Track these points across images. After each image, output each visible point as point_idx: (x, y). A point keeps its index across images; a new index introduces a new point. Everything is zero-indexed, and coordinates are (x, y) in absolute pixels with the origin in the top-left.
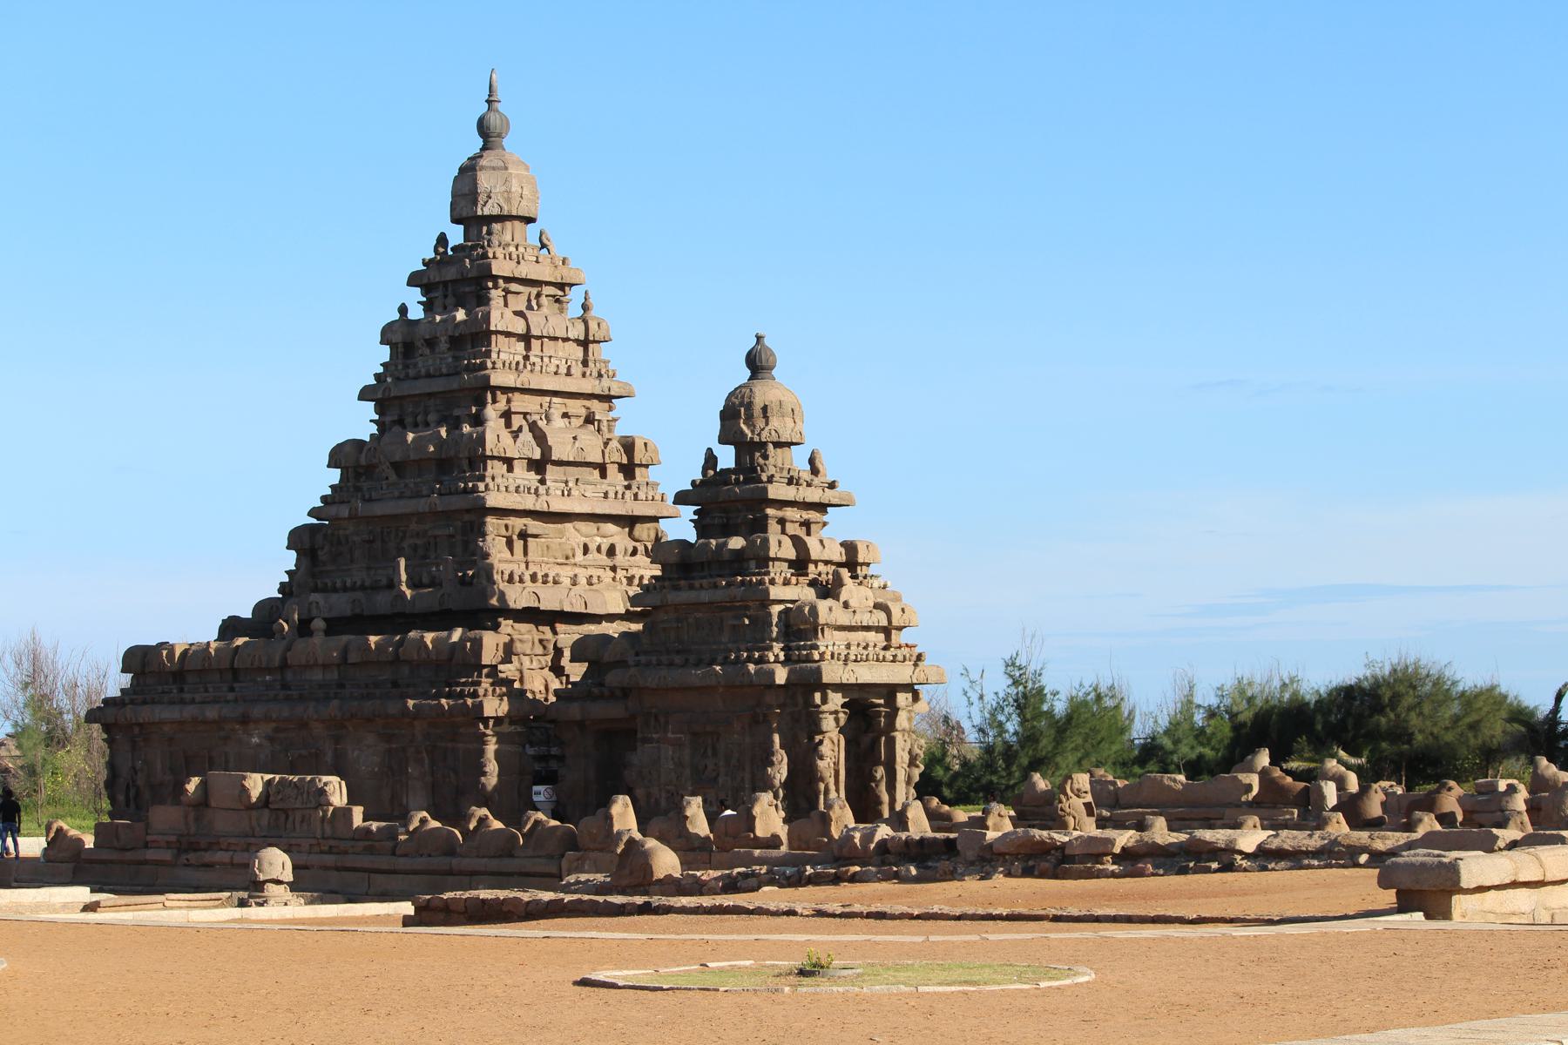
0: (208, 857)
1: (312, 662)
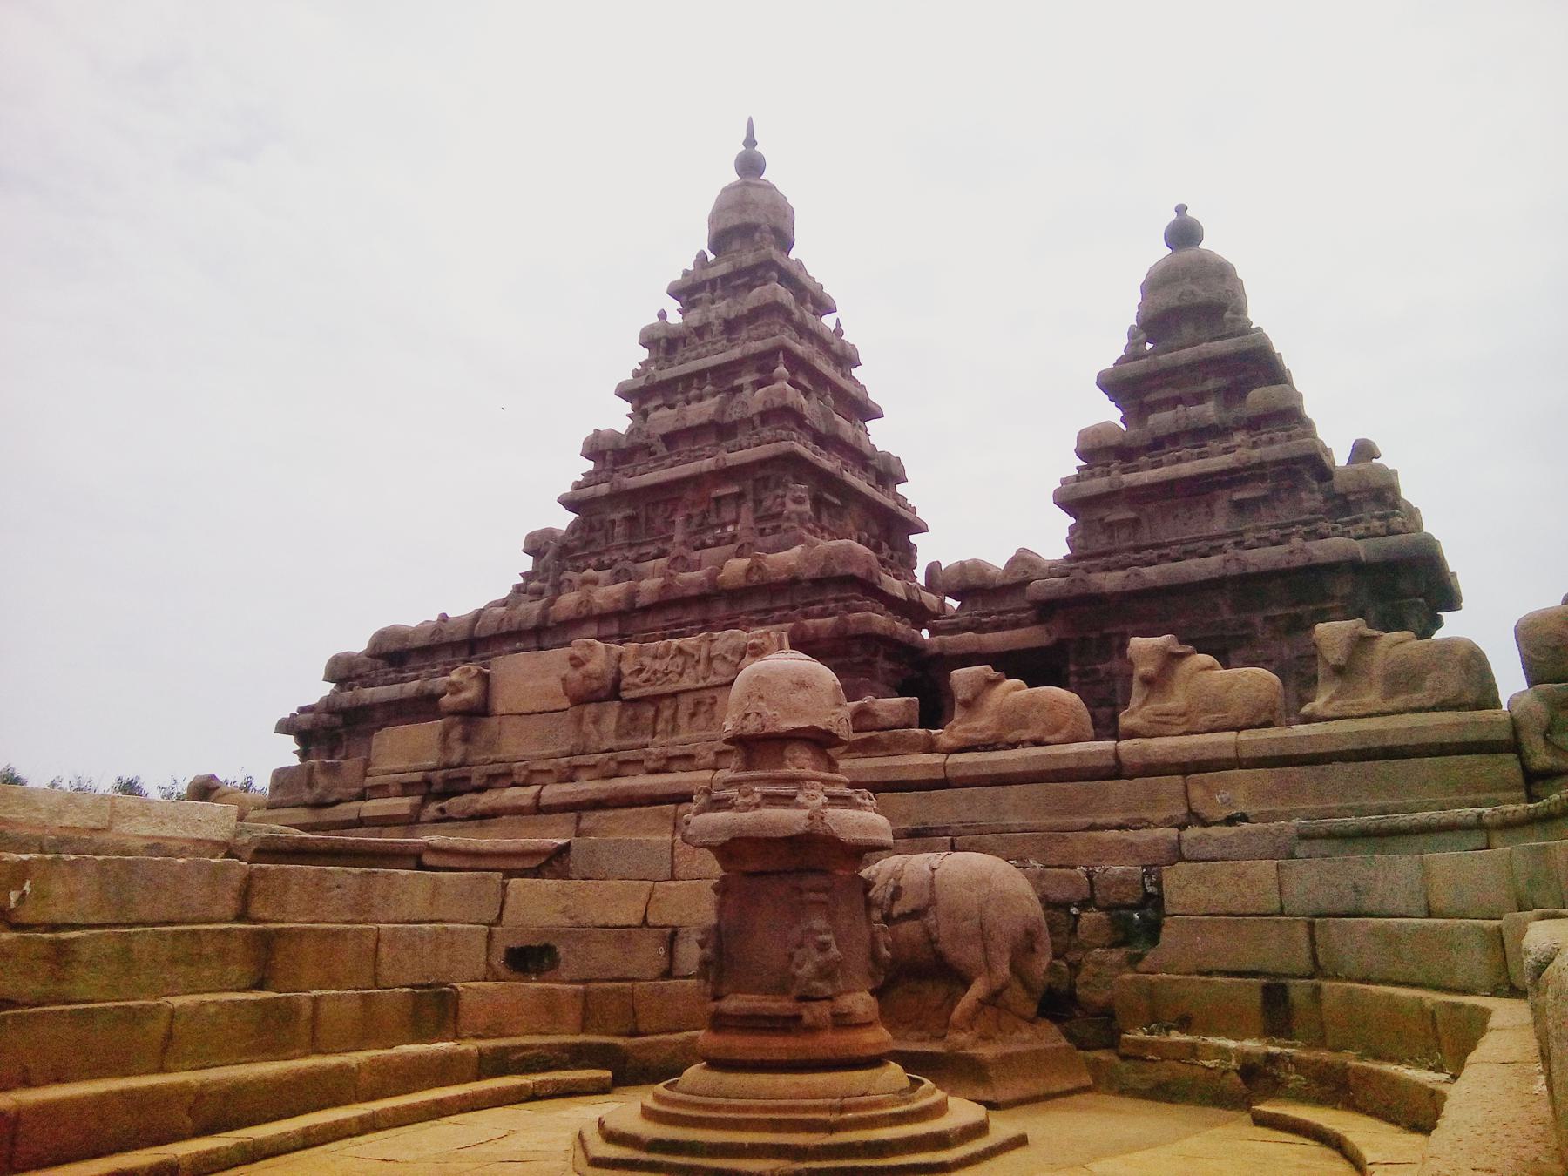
0: (486, 800)
1: (584, 611)
